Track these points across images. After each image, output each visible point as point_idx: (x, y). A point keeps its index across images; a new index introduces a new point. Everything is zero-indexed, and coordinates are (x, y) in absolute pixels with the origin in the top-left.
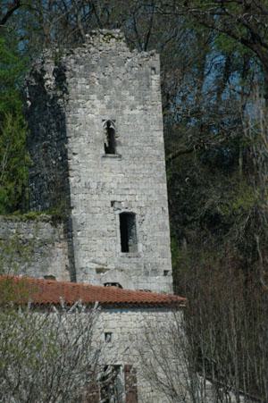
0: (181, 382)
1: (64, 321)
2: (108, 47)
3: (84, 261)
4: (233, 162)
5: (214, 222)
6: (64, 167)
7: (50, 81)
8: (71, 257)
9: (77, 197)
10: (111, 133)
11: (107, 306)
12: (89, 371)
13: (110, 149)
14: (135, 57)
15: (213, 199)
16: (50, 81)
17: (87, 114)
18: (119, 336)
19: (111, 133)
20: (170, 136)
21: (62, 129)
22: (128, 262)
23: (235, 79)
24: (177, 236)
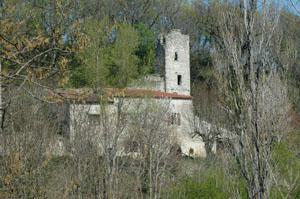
0: (191, 118)
1: (163, 102)
2: (176, 34)
3: (168, 87)
4: (206, 64)
5: (201, 79)
6: (164, 63)
7: (162, 41)
8: (165, 85)
9: (167, 70)
10: (176, 55)
11: (173, 98)
12: (169, 114)
13: (176, 59)
14: (183, 36)
15: (201, 73)
16: (162, 41)
17: (170, 50)
18: (176, 106)
19: (176, 55)
20: (191, 56)
21: (164, 54)
22: (179, 87)
23: (208, 43)
24: (192, 81)
